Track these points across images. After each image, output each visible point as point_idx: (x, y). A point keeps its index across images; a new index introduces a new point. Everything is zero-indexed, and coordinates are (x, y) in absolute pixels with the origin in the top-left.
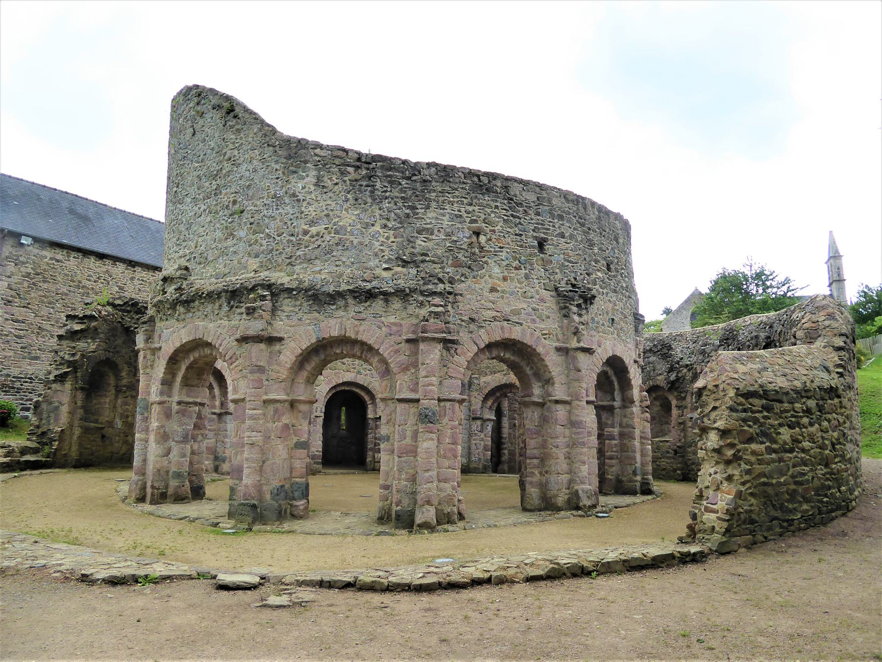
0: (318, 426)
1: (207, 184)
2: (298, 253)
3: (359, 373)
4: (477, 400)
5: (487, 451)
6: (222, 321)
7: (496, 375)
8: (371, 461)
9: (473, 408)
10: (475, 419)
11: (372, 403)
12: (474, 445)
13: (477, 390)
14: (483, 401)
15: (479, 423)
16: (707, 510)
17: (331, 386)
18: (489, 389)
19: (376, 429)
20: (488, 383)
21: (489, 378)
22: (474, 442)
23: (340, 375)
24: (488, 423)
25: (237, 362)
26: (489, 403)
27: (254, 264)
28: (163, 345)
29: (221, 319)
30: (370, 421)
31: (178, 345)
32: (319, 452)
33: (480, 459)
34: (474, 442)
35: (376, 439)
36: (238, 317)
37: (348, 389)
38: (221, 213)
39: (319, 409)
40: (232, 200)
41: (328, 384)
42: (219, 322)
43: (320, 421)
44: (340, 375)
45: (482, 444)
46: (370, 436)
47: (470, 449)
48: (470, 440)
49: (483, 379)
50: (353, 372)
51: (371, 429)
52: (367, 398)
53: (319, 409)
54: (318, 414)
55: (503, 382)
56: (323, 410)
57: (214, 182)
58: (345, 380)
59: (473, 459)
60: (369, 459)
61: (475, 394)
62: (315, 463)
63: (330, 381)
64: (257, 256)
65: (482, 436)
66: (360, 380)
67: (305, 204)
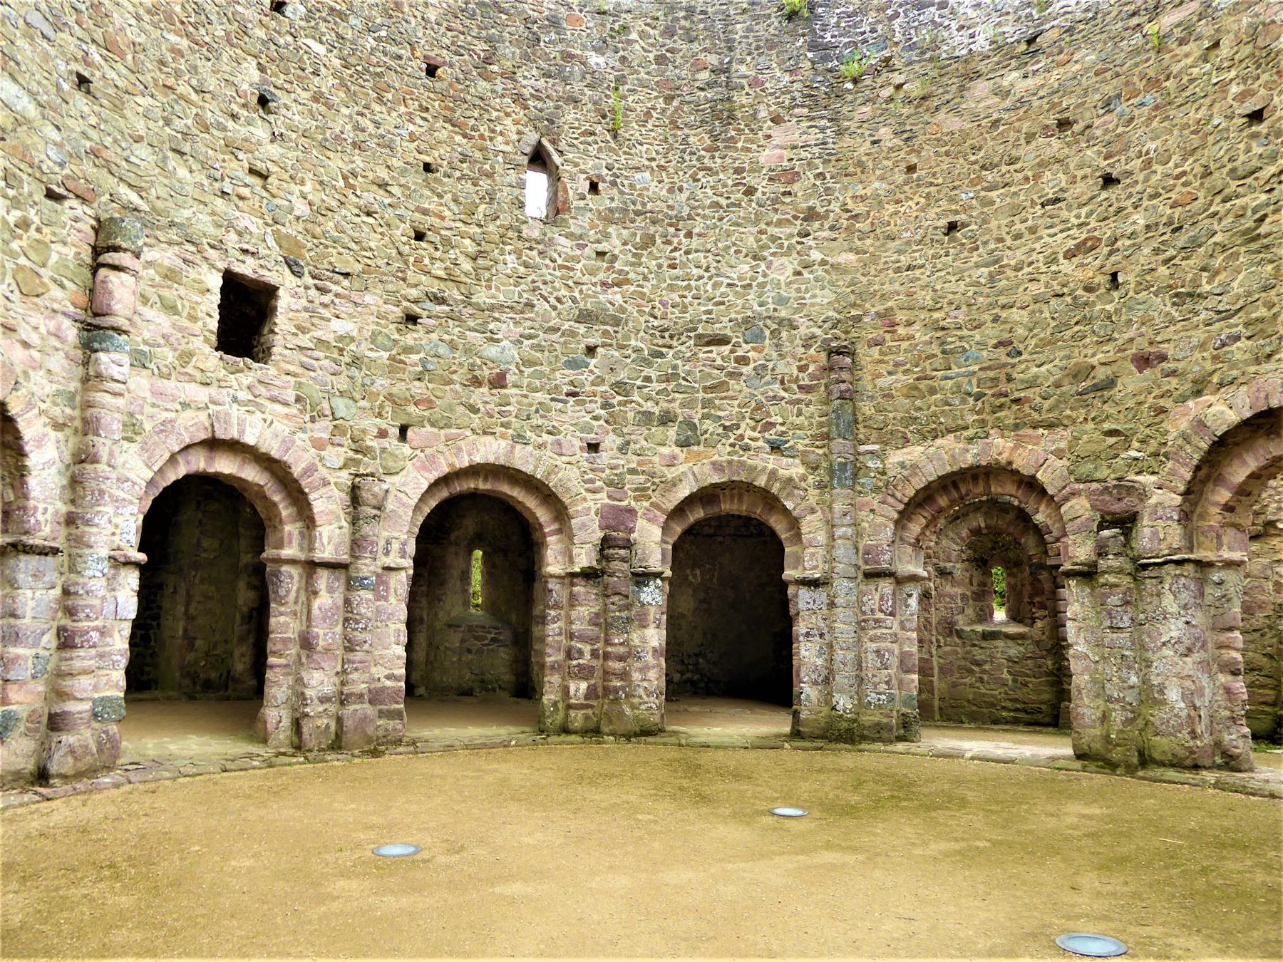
0: (392, 599)
3: (519, 438)
4: (880, 520)
5: (907, 672)
7: (939, 442)
8: (555, 704)
9: (867, 541)
10: (871, 576)
11: (559, 531)
12: (871, 656)
13: (877, 489)
14: (897, 522)
15: (886, 586)
17: (434, 476)
18: (919, 482)
19: (572, 606)
20: (915, 467)
21: (914, 453)
22: (874, 646)
23: (462, 444)
24: (909, 588)
26: (915, 528)
30: (553, 585)
32: (396, 678)
33: (891, 699)
34: (874, 646)
35: (571, 636)
37: (488, 486)
39: (396, 546)
41: (425, 468)
43: (400, 584)
44: (462, 444)
45: (896, 652)
46: (552, 628)
47: (860, 667)
48: (859, 641)
49: (896, 457)
50: (503, 436)
51: (557, 606)
52: (542, 515)
53: (396, 546)
54: (392, 560)
55: (969, 460)
56: (411, 548)
58: (478, 459)
59: (873, 697)
60: (549, 697)
61: (873, 500)
62: (381, 714)
63: (432, 460)
65: (896, 628)
66: (524, 460)
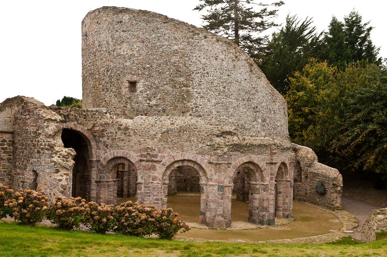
1: (243, 94)
2: (275, 132)
6: (260, 155)
16: (336, 203)
25: (266, 171)
27: (263, 134)
28: (233, 162)
29: (259, 154)
31: (242, 163)
36: (265, 155)
38: (251, 110)
40: (256, 106)
42: (259, 155)
57: (246, 95)
64: (264, 131)
67: (276, 114)
